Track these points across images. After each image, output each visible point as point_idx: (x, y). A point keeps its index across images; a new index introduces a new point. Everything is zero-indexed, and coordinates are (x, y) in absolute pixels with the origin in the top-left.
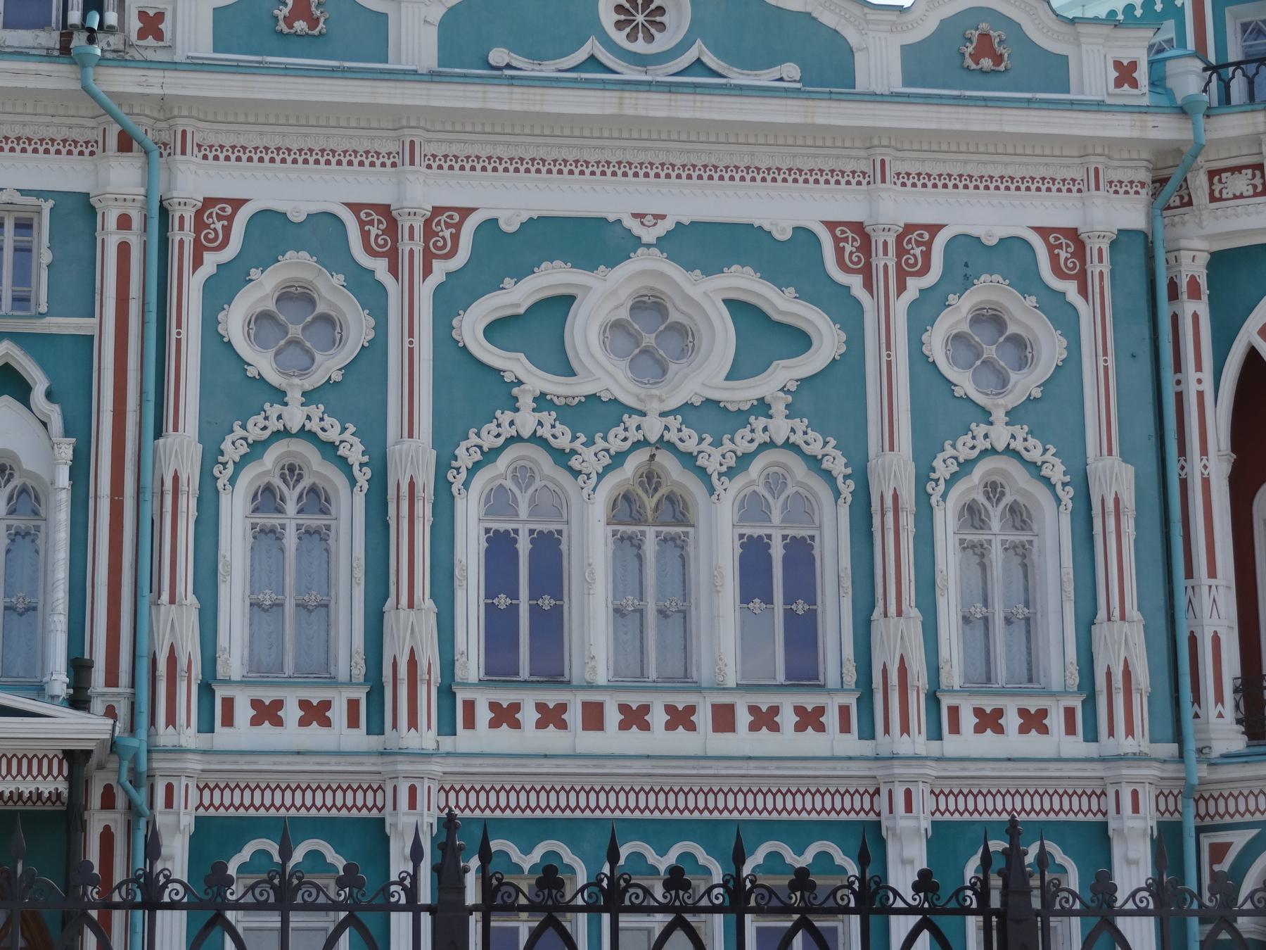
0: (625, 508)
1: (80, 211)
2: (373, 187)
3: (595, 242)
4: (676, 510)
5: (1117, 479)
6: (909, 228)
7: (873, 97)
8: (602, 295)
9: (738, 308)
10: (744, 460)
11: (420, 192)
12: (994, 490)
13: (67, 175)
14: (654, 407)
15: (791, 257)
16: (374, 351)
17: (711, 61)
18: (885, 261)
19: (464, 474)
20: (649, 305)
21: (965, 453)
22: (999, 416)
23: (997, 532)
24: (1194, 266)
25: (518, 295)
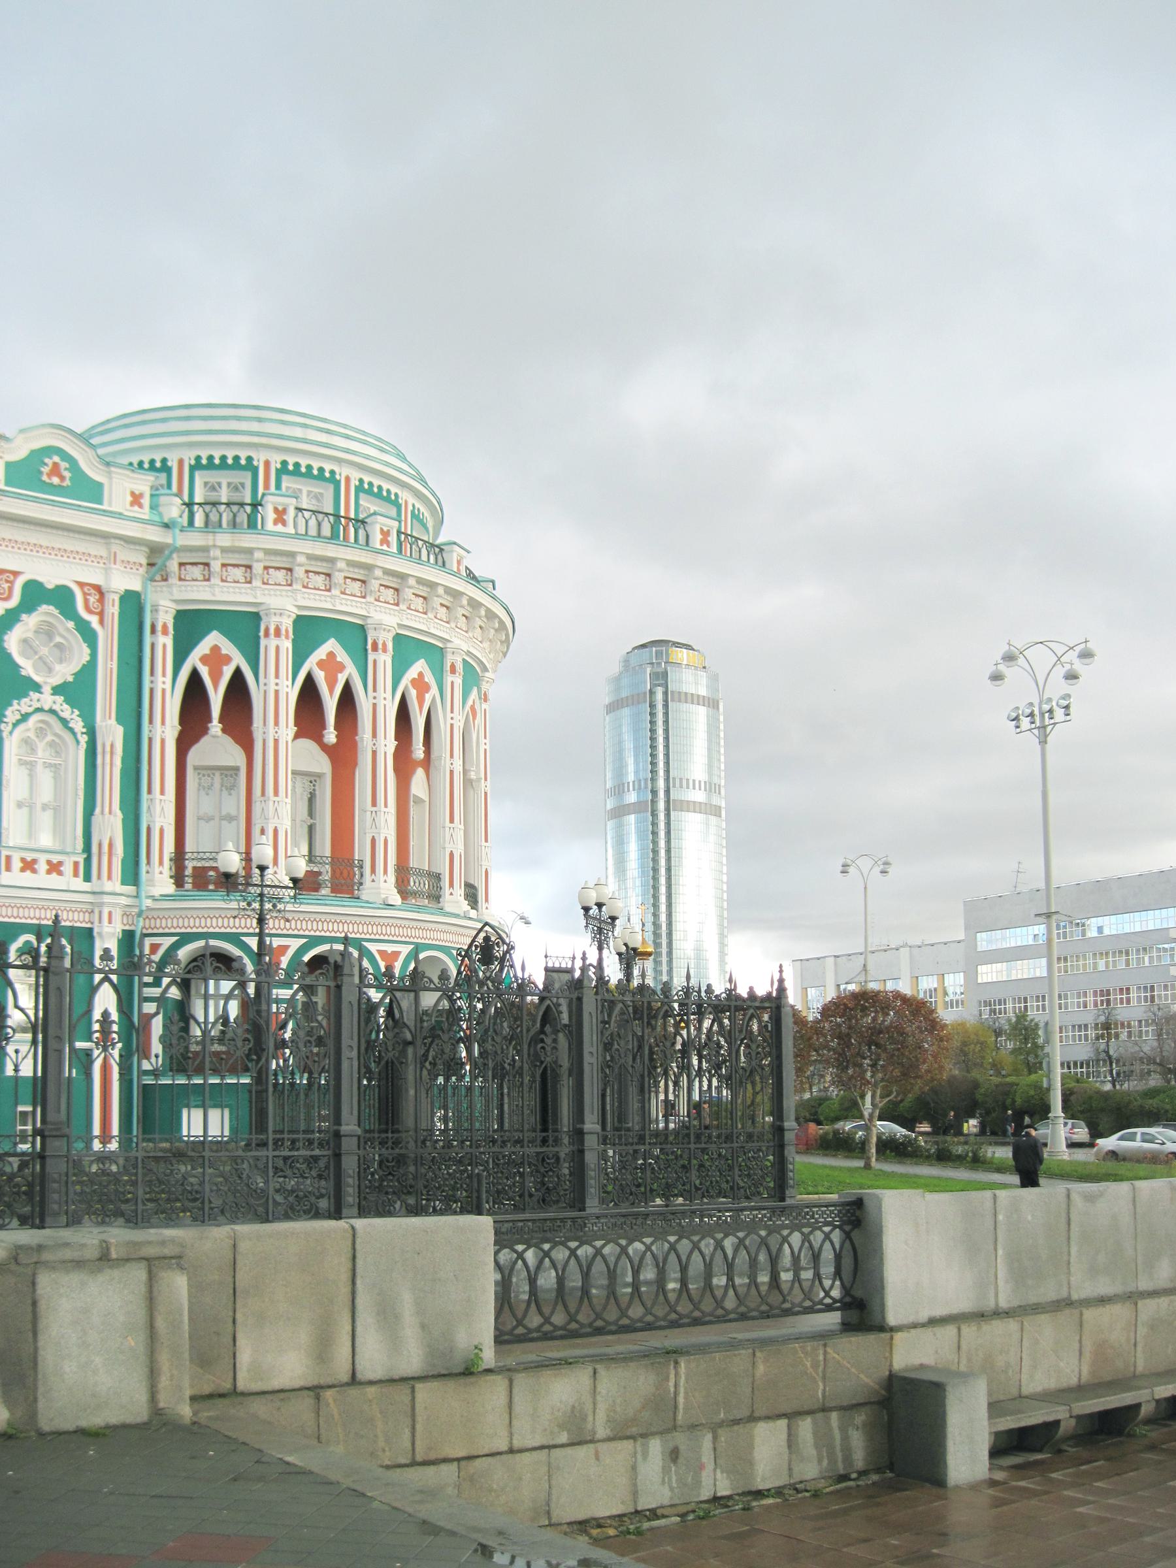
5: (112, 734)
19: (10, 727)
21: (25, 709)
22: (47, 689)
24: (166, 618)
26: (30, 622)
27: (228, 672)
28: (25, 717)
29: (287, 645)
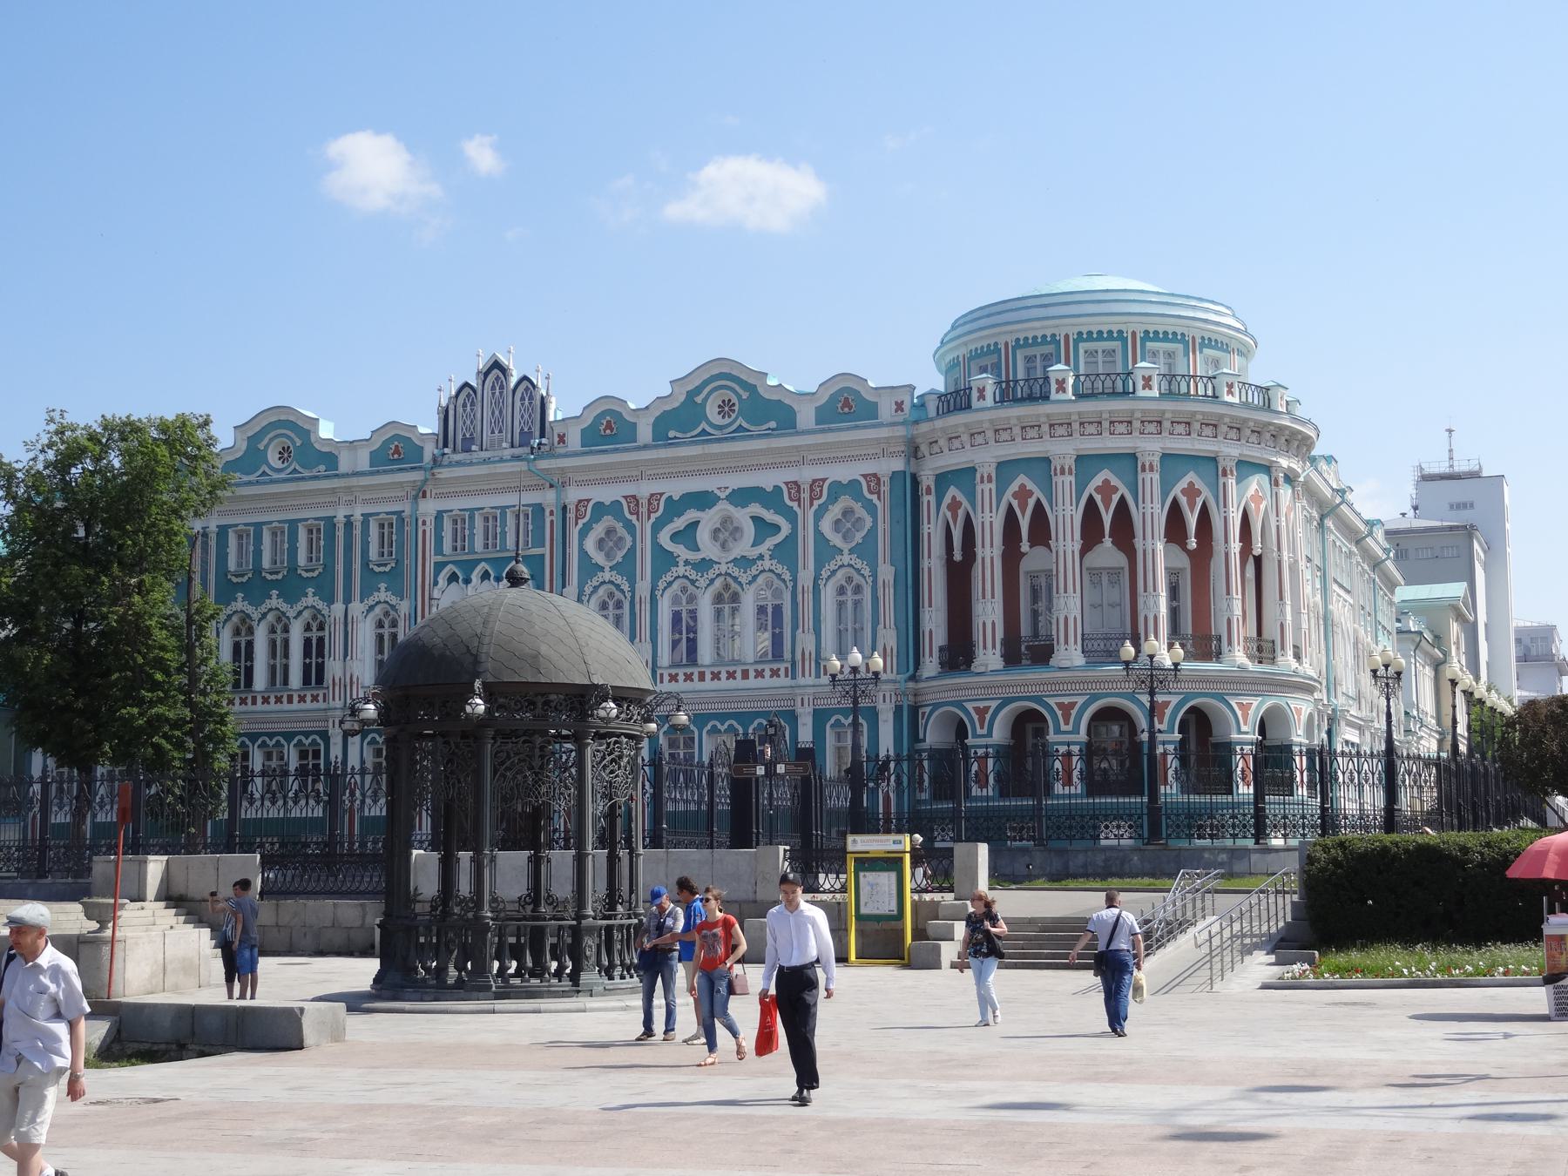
0: (718, 599)
1: (539, 509)
2: (629, 489)
3: (703, 500)
4: (735, 598)
5: (886, 572)
6: (814, 481)
7: (804, 433)
8: (708, 520)
9: (757, 520)
10: (755, 577)
11: (644, 490)
12: (849, 579)
13: (530, 498)
14: (724, 561)
15: (770, 498)
16: (632, 549)
17: (745, 425)
18: (806, 495)
20: (726, 520)
21: (833, 567)
22: (846, 552)
23: (849, 597)
25: (679, 523)
26: (835, 511)
27: (961, 513)
28: (834, 572)
29: (993, 486)
